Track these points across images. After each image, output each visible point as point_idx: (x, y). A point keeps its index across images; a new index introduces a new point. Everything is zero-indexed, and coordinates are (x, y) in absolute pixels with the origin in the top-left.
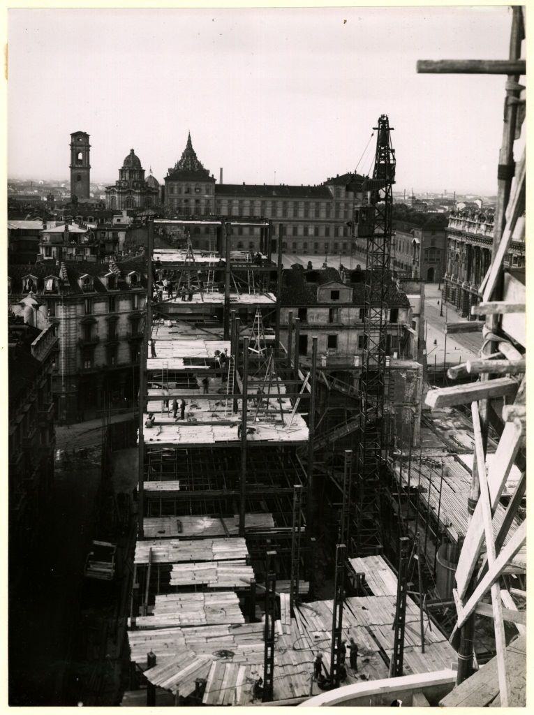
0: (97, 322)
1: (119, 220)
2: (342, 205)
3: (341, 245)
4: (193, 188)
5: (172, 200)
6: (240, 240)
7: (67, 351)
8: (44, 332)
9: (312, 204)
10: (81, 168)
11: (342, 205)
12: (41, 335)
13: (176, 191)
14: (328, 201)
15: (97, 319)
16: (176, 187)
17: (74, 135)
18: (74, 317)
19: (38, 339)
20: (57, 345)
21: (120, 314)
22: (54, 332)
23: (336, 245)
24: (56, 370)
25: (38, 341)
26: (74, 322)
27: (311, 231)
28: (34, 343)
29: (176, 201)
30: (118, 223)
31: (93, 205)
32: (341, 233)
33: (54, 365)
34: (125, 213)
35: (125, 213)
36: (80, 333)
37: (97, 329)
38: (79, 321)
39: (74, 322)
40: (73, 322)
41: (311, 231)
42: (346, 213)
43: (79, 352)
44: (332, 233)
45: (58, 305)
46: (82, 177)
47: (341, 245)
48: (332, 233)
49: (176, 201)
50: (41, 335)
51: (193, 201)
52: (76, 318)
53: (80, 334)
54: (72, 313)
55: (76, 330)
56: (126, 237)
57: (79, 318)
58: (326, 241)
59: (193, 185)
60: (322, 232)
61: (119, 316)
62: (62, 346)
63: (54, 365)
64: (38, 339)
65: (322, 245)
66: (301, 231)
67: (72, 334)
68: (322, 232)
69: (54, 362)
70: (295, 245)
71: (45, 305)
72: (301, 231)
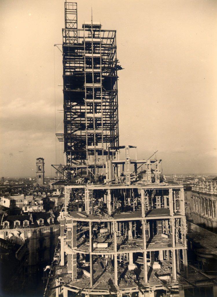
0: (45, 239)
1: (55, 193)
7: (33, 253)
8: (21, 246)
10: (40, 172)
12: (20, 248)
15: (46, 238)
17: (38, 159)
18: (35, 238)
19: (19, 250)
20: (28, 251)
21: (55, 235)
22: (27, 246)
24: (28, 263)
25: (19, 251)
26: (36, 240)
28: (17, 252)
30: (55, 195)
31: (45, 187)
33: (27, 260)
34: (58, 190)
35: (58, 190)
36: (38, 245)
37: (46, 243)
38: (38, 239)
39: (36, 240)
40: (35, 240)
43: (37, 254)
45: (29, 233)
46: (41, 176)
50: (20, 248)
52: (36, 238)
53: (38, 246)
54: (35, 236)
55: (37, 244)
56: (58, 200)
57: (38, 238)
61: (54, 236)
62: (30, 252)
63: (27, 260)
64: (19, 250)
67: (35, 246)
69: (27, 259)
71: (23, 233)
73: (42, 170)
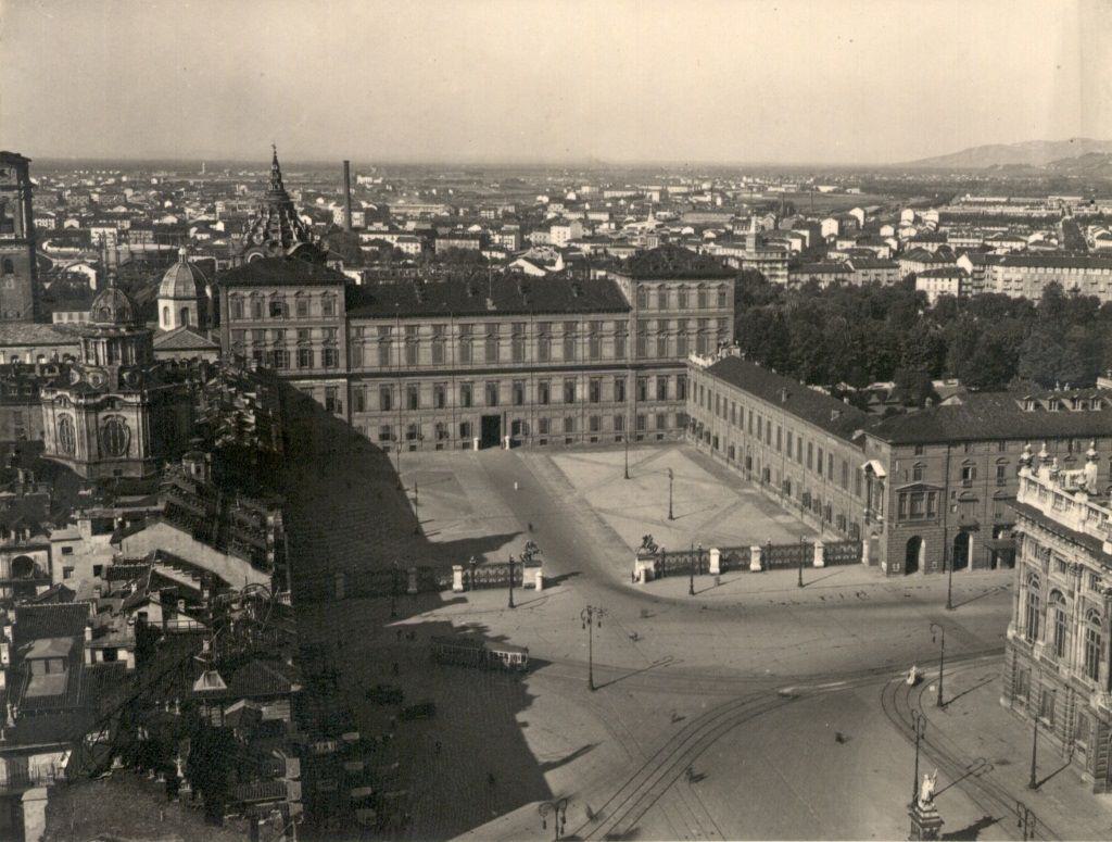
2: (653, 325)
3: (651, 420)
4: (291, 302)
5: (241, 332)
6: (413, 420)
9: (583, 326)
11: (653, 325)
13: (247, 311)
14: (620, 317)
16: (248, 301)
23: (640, 420)
27: (582, 392)
29: (249, 335)
32: (652, 391)
41: (582, 392)
42: (661, 344)
44: (630, 391)
47: (651, 420)
48: (630, 391)
49: (249, 335)
51: (292, 334)
58: (618, 411)
59: (289, 295)
60: (608, 392)
65: (608, 422)
66: (557, 394)
68: (608, 392)
70: (544, 426)
72: (557, 394)
73: (17, 227)
